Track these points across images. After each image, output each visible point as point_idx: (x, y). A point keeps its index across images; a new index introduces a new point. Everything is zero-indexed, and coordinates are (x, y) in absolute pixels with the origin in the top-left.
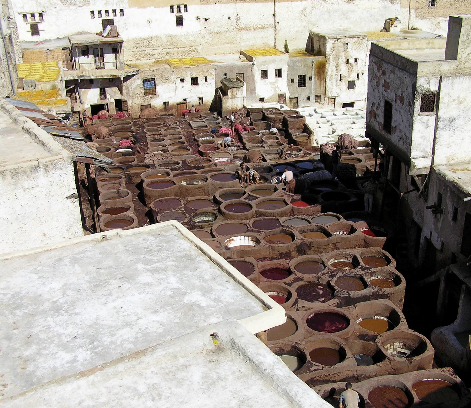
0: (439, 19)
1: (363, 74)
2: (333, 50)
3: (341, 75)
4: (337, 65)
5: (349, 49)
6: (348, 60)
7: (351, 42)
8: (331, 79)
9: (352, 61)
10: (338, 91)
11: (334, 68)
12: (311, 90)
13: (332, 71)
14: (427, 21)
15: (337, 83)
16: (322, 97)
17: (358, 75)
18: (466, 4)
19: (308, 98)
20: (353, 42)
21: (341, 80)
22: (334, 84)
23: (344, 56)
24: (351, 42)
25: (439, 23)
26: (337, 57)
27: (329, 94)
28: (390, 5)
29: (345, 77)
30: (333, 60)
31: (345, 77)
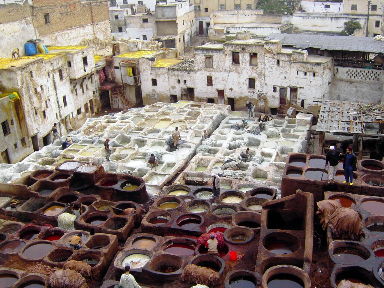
0: (56, 34)
1: (49, 100)
2: (22, 82)
3: (35, 107)
4: (30, 98)
5: (34, 78)
6: (36, 89)
7: (33, 68)
8: (29, 116)
9: (39, 89)
10: (37, 126)
11: (28, 102)
12: (15, 136)
13: (28, 106)
14: (48, 38)
15: (34, 118)
16: (26, 138)
17: (46, 102)
18: (69, 17)
19: (16, 146)
20: (35, 69)
21: (36, 114)
22: (33, 120)
23: (32, 86)
24: (33, 68)
25: (56, 38)
26: (28, 89)
27: (32, 134)
28: (26, 26)
29: (38, 109)
30: (26, 95)
31: (38, 109)
